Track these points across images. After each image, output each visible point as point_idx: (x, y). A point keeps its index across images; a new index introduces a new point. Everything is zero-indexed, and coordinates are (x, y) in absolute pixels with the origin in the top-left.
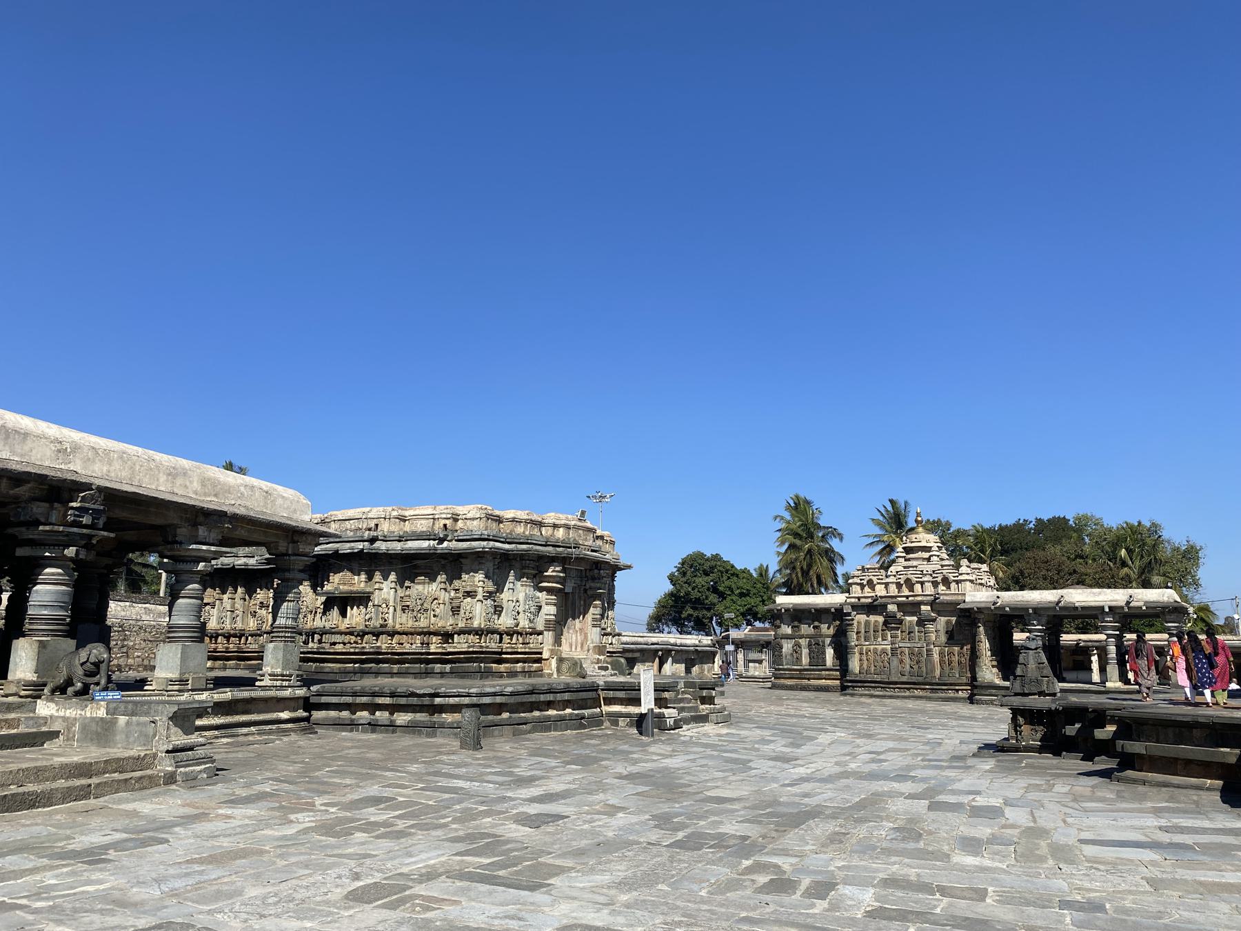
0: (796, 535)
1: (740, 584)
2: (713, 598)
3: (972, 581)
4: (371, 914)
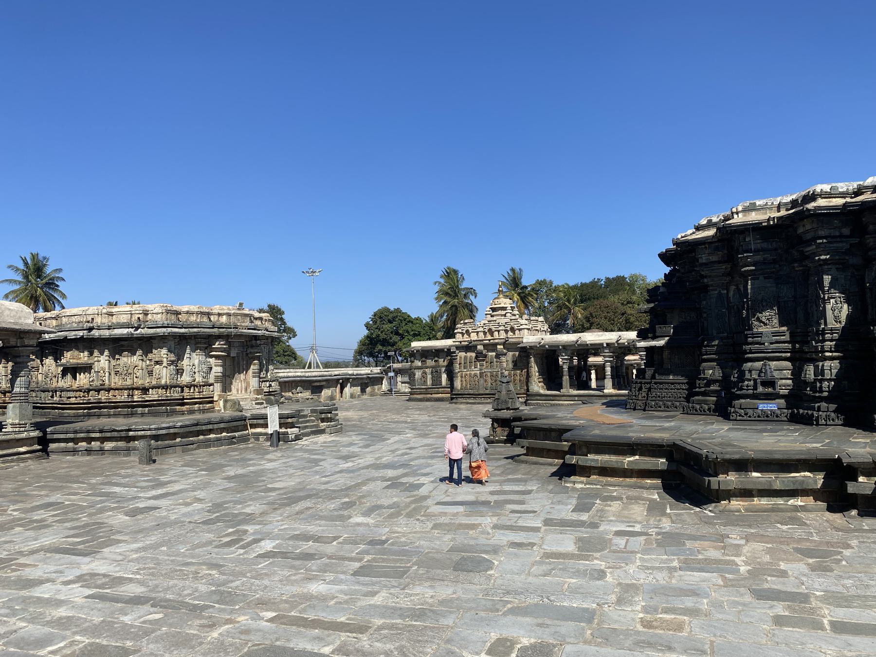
0: (447, 294)
2: (396, 338)
3: (528, 329)
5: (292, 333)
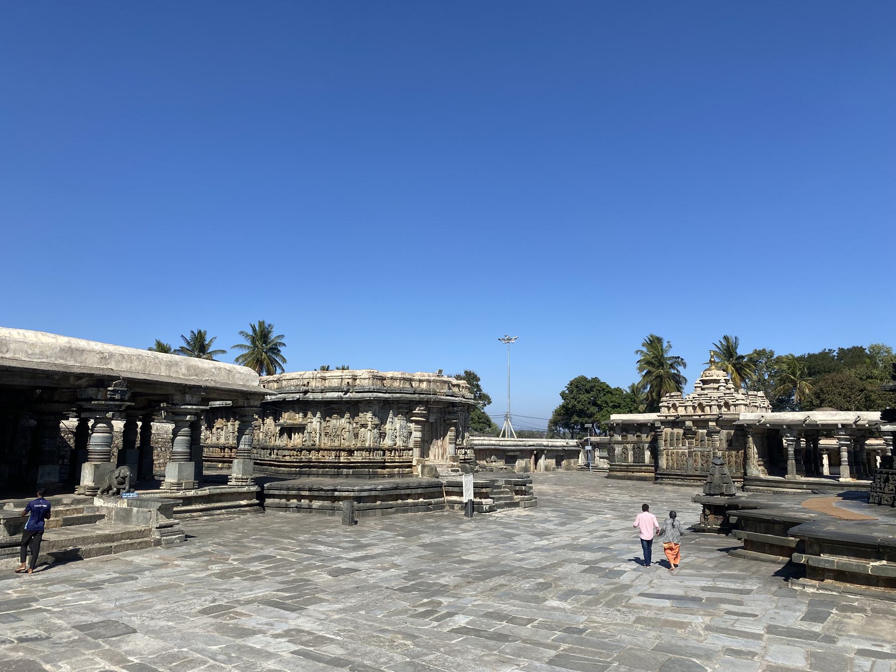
0: (649, 363)
1: (613, 399)
2: (593, 409)
4: (207, 619)
5: (486, 399)
